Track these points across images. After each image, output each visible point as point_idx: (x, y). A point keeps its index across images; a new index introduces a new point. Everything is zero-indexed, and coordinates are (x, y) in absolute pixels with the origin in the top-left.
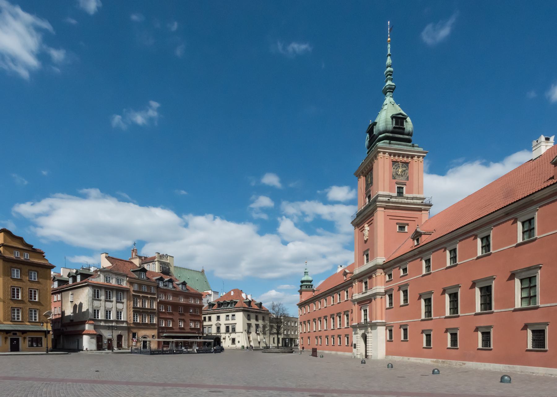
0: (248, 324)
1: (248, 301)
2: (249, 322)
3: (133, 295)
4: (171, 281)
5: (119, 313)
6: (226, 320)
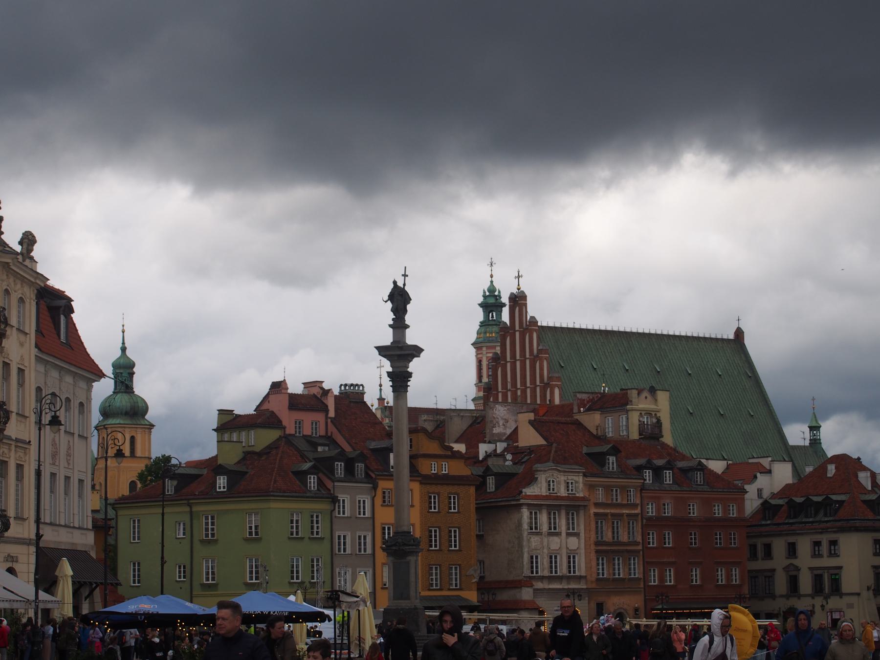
1: (873, 497)
3: (596, 514)
5: (571, 558)
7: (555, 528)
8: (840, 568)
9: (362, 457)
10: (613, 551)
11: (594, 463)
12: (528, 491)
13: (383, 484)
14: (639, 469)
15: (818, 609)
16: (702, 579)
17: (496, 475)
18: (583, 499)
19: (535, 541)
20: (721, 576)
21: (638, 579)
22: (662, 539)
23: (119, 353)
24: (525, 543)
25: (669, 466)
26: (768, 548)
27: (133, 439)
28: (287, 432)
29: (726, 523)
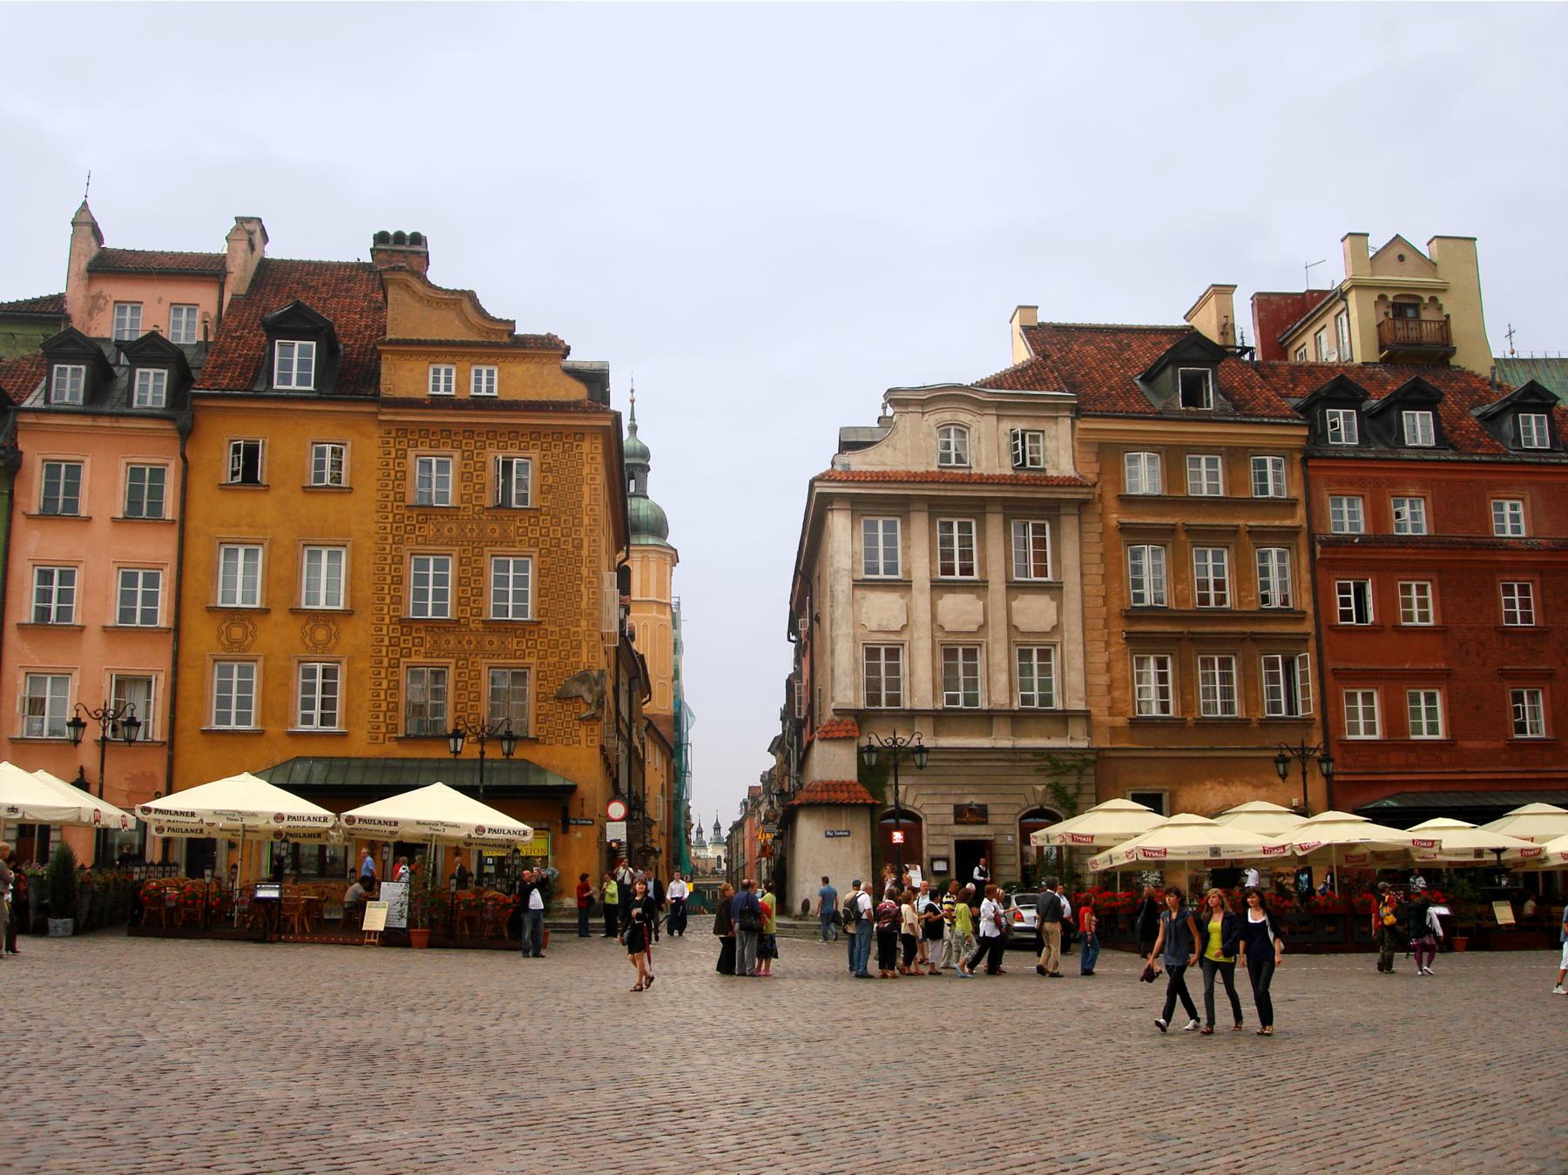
3: (1124, 529)
7: (966, 570)
10: (1195, 639)
21: (1307, 723)
25: (1421, 398)
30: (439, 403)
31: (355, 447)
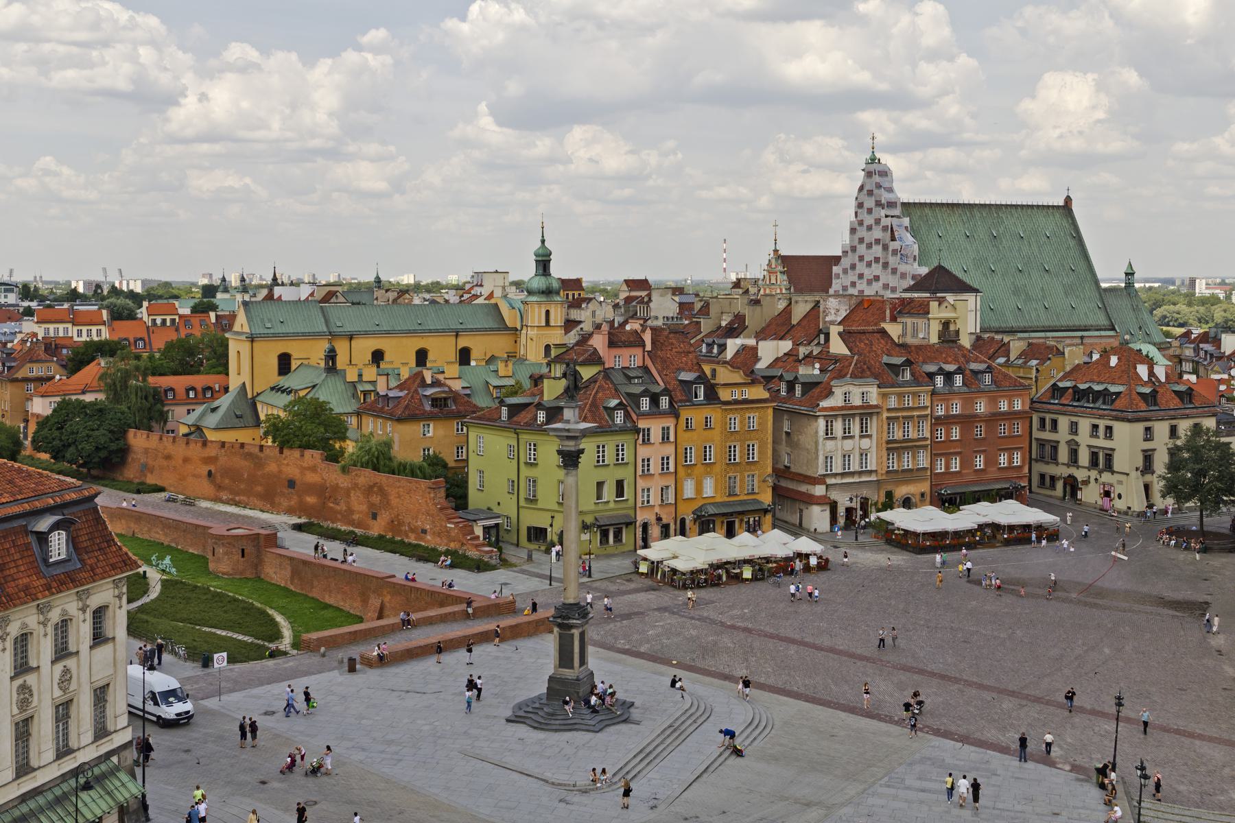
0: (1144, 451)
1: (1147, 390)
2: (1148, 445)
3: (888, 418)
4: (960, 371)
5: (863, 454)
6: (1092, 436)
8: (1113, 450)
9: (666, 392)
11: (887, 376)
12: (824, 404)
13: (685, 414)
14: (931, 376)
15: (1092, 480)
16: (986, 464)
17: (803, 384)
18: (876, 407)
19: (830, 444)
20: (1003, 460)
22: (948, 434)
23: (540, 244)
24: (820, 447)
25: (960, 371)
26: (1055, 423)
27: (548, 312)
28: (607, 366)
29: (1011, 416)
30: (736, 402)
31: (714, 413)
